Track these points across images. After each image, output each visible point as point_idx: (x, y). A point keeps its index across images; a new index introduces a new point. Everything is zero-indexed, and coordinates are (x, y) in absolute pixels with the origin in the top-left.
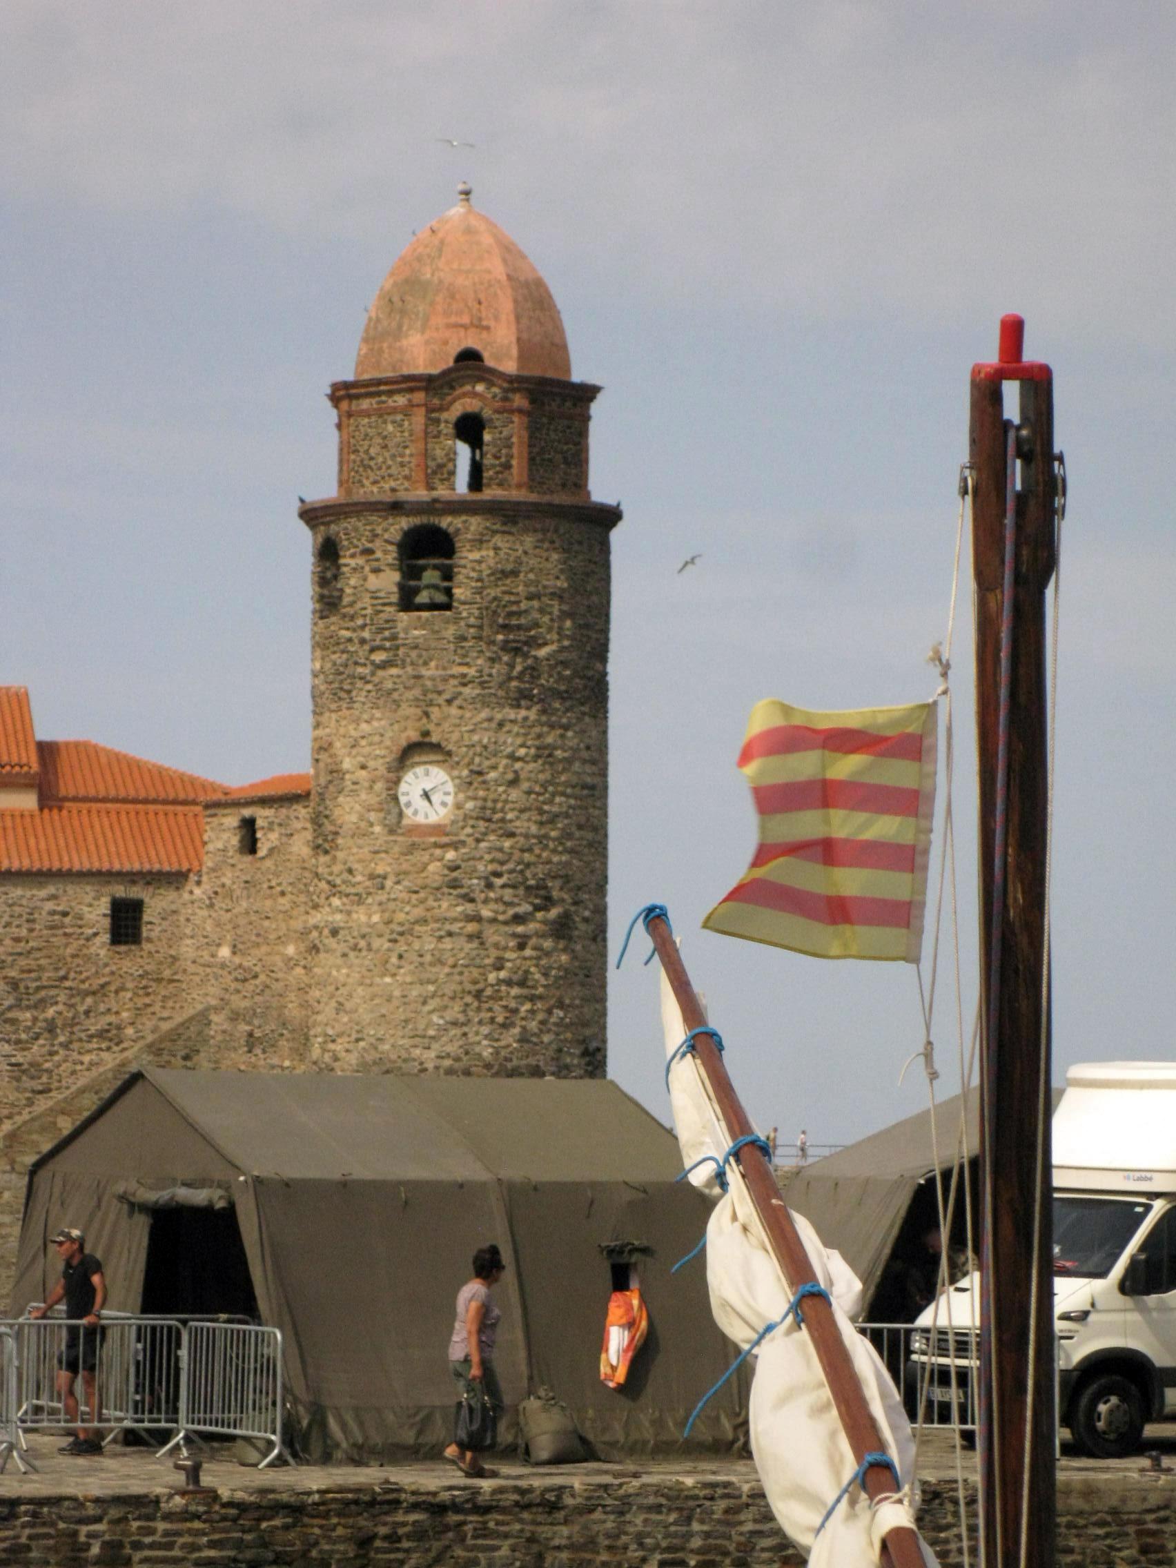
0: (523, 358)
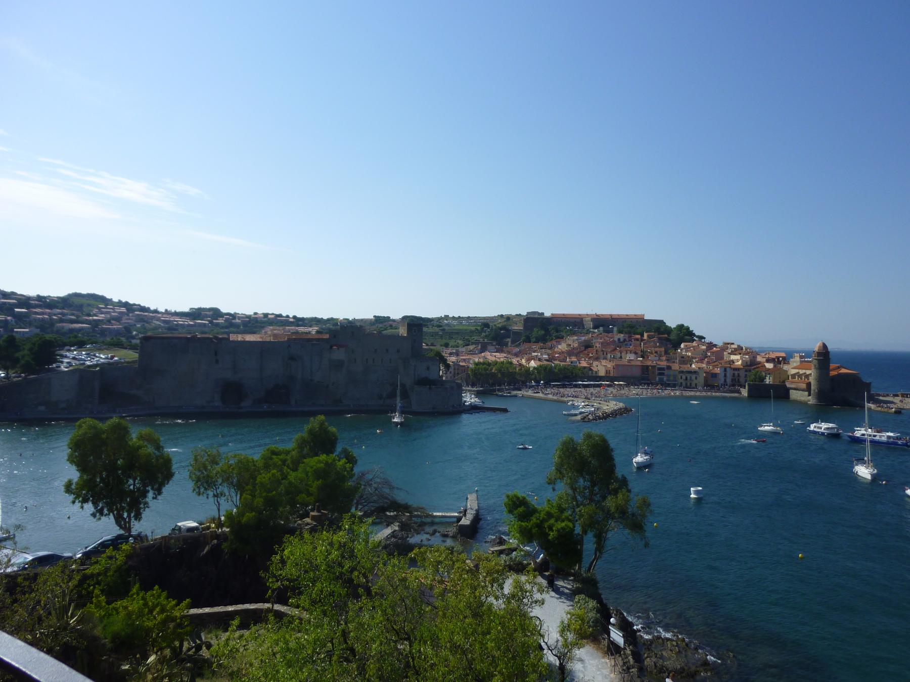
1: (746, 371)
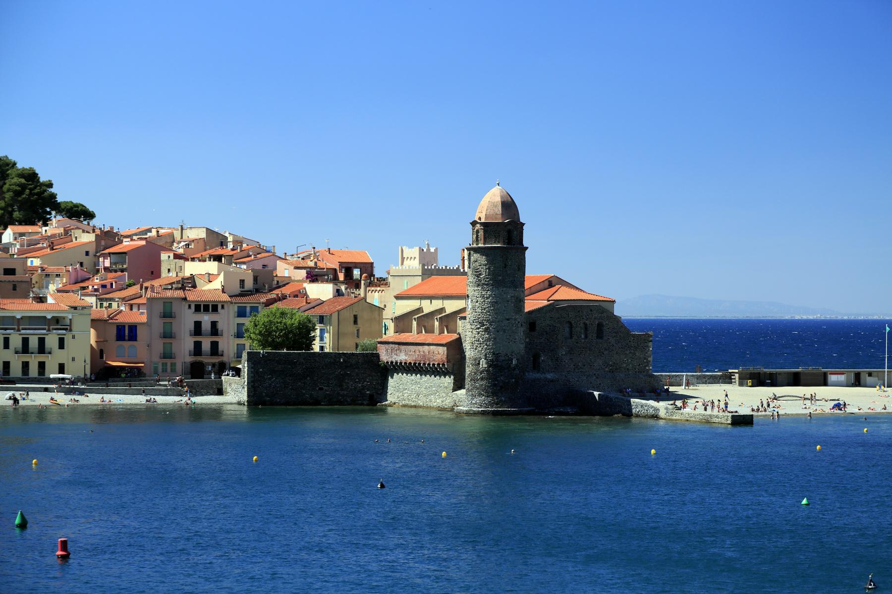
0: (486, 218)
1: (241, 313)
